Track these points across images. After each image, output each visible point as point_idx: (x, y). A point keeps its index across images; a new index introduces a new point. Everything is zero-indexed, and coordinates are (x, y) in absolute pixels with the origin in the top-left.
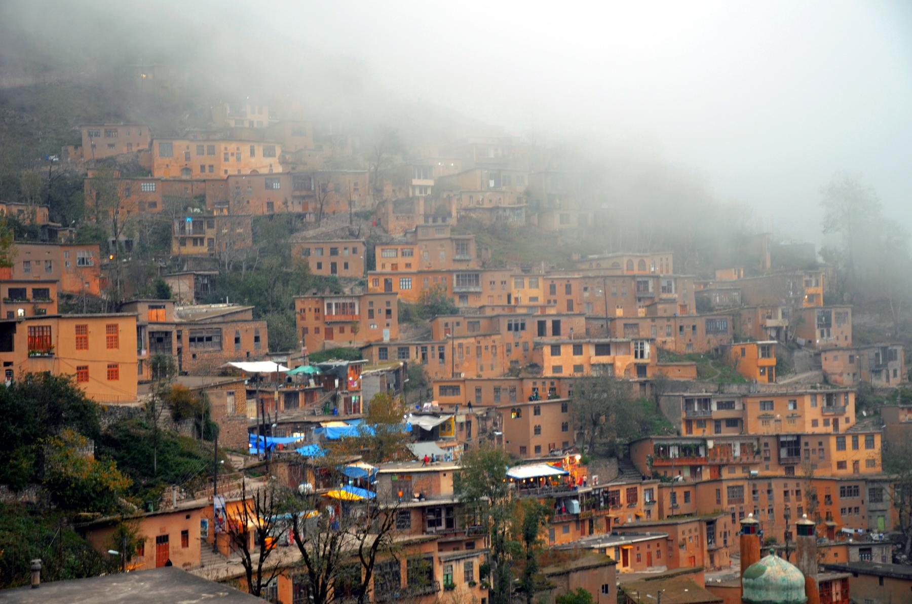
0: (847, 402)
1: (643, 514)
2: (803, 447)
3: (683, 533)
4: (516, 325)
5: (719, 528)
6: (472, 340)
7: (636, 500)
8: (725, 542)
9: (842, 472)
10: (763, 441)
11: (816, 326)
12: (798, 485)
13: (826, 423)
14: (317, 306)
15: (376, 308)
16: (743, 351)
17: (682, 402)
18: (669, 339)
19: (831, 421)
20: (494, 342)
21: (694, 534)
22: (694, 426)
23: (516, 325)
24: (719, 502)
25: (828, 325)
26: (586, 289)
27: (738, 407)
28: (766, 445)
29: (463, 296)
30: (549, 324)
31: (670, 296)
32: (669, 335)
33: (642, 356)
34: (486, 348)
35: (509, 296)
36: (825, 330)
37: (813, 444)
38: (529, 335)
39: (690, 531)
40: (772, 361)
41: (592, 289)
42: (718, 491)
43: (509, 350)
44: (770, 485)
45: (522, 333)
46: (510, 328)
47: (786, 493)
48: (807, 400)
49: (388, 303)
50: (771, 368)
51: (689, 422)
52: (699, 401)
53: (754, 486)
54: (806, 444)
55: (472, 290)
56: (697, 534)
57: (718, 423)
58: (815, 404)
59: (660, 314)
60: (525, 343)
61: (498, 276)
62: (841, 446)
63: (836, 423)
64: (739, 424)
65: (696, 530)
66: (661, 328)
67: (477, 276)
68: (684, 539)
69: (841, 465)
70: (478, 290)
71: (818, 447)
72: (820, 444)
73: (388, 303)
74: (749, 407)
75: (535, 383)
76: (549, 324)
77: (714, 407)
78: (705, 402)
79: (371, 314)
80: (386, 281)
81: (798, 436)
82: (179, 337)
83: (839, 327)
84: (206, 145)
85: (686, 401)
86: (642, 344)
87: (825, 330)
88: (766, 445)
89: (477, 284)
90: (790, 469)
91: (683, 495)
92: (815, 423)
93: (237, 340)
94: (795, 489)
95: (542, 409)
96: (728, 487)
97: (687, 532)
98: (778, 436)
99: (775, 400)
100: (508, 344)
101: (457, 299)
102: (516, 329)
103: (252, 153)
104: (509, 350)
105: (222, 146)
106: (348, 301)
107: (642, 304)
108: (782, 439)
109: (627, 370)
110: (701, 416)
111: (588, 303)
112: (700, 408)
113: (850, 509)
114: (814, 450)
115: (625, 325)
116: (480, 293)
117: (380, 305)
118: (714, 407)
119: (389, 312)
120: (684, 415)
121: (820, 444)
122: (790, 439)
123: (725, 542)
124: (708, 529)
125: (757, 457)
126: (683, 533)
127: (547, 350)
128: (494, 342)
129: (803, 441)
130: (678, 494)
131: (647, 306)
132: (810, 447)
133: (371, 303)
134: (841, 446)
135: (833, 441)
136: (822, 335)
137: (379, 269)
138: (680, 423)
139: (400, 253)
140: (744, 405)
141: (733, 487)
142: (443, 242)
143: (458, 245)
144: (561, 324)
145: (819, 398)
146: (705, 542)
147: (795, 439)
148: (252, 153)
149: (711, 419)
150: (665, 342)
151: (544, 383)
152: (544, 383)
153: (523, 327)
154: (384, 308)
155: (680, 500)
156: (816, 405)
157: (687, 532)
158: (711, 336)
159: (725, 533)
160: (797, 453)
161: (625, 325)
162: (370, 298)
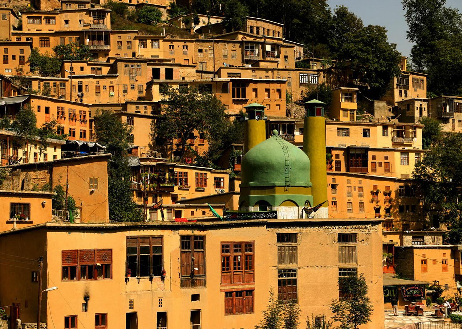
7: (206, 186)
11: (395, 86)
12: (360, 182)
20: (112, 83)
25: (406, 87)
26: (200, 51)
28: (338, 156)
34: (105, 87)
36: (403, 91)
41: (206, 51)
43: (125, 91)
48: (380, 128)
50: (352, 111)
54: (374, 157)
60: (141, 85)
61: (125, 37)
71: (383, 161)
72: (386, 158)
75: (137, 107)
87: (403, 91)
88: (338, 156)
104: (125, 91)
111: (201, 63)
115: (228, 74)
116: (109, 51)
121: (386, 158)
128: (112, 83)
129: (370, 154)
132: (377, 161)
136: (400, 95)
144: (174, 72)
151: (146, 107)
152: (146, 107)
158: (303, 88)
161: (228, 74)
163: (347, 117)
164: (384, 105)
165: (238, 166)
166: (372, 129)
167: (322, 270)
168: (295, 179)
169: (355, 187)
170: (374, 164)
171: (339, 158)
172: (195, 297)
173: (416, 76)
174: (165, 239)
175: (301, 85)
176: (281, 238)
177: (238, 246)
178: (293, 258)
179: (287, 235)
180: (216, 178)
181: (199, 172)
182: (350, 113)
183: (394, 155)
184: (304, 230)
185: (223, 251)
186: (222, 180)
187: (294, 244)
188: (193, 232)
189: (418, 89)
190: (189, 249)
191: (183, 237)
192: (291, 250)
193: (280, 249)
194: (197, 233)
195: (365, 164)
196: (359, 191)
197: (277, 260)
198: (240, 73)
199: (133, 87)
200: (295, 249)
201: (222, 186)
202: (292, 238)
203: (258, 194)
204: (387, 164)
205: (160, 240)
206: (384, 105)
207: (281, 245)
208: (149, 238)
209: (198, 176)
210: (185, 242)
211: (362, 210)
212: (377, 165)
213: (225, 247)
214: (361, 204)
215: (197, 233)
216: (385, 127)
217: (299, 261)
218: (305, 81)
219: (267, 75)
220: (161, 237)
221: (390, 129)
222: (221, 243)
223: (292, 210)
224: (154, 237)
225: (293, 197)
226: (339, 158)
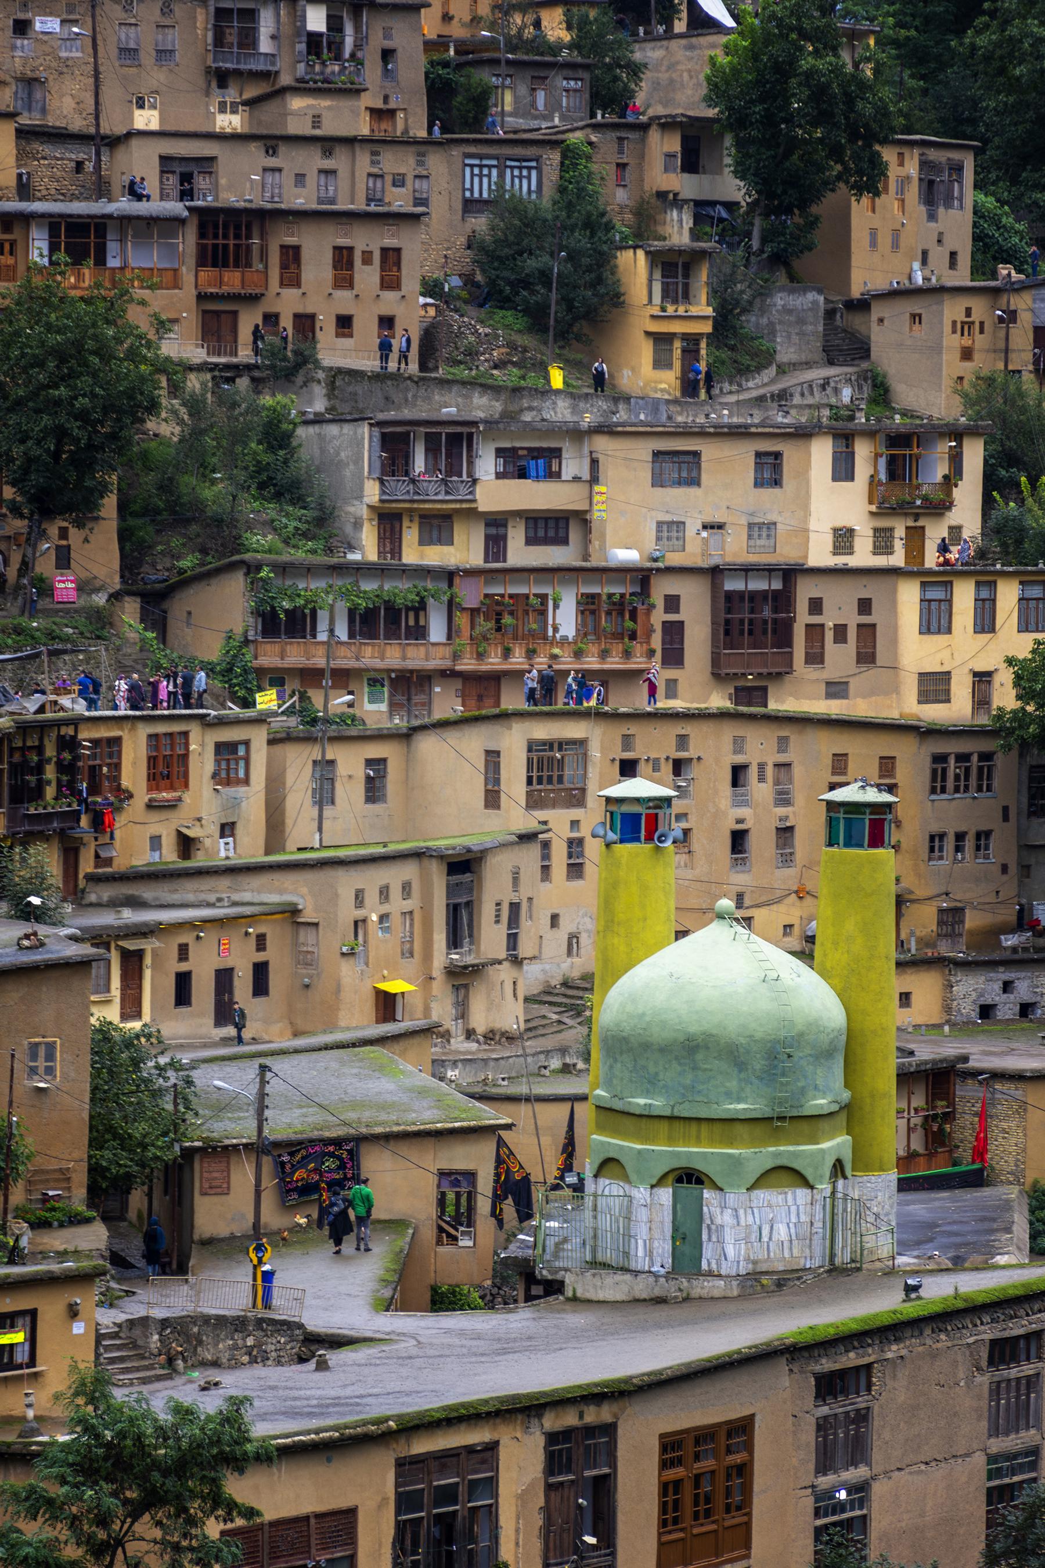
1: (206, 832)
2: (803, 617)
3: (359, 898)
5: (495, 887)
8: (513, 940)
9: (934, 713)
10: (661, 588)
13: (883, 542)
19: (900, 532)
21: (397, 904)
22: (410, 535)
24: (492, 799)
27: (572, 465)
37: (840, 607)
39: (384, 893)
42: (493, 758)
44: (682, 741)
47: (738, 773)
48: (821, 453)
50: (691, 342)
51: (389, 522)
53: (627, 741)
54: (816, 606)
56: (408, 905)
57: (496, 527)
58: (843, 470)
59: (294, 127)
62: (936, 620)
63: (916, 537)
64: (574, 535)
65: (406, 889)
68: (358, 924)
69: (935, 686)
71: (853, 620)
72: (865, 606)
74: (609, 470)
77: (486, 465)
81: (791, 573)
83: (932, 217)
85: (384, 436)
88: (672, 603)
90: (750, 694)
91: (360, 772)
92: (843, 539)
94: (772, 758)
96: (532, 746)
97: (372, 897)
98: (715, 573)
99: (710, 451)
107: (231, 95)
108: (734, 585)
110: (435, 496)
112: (432, 468)
114: (840, 632)
118: (486, 465)
120: (372, 492)
121: (865, 606)
122: (758, 585)
123: (513, 940)
124: (451, 890)
125: (638, 648)
126: (359, 898)
129: (805, 591)
130: (342, 769)
131: (250, 103)
132: (829, 620)
134: (936, 620)
135: (909, 596)
138: (358, 525)
140: (594, 463)
141: (549, 745)
146: (440, 938)
147: (777, 585)
149: (472, 514)
155: (350, 789)
156: (850, 476)
157: (372, 897)
158: (480, 223)
159: (515, 907)
163: (669, 366)
164: (815, 303)
165: (268, 647)
166: (790, 452)
167: (938, 1472)
168: (803, 1091)
169: (762, 767)
170: (815, 632)
171: (677, 611)
173: (933, 154)
175: (470, 206)
176: (829, 1386)
177: (703, 1436)
178: (858, 1451)
179: (842, 1373)
180: (219, 747)
181: (161, 728)
182: (684, 351)
183: (894, 592)
184: (893, 1351)
185: (665, 1465)
186: (241, 752)
187: (861, 1402)
188: (581, 1416)
189: (941, 210)
190: (569, 1471)
191: (552, 1438)
192: (853, 1422)
193: (823, 1426)
194: (593, 1415)
195: (783, 635)
196: (777, 782)
197: (812, 1466)
198: (212, 159)
200: (862, 1417)
201: (241, 774)
202: (857, 1378)
203: (671, 1140)
204: (867, 631)
205: (489, 1453)
206: (815, 303)
207: (825, 1410)
208: (458, 1455)
209: (157, 748)
210: (560, 1451)
211: (787, 859)
212: (829, 636)
214: (785, 832)
215: (593, 1415)
216: (845, 440)
217: (876, 1455)
218: (483, 189)
219: (328, 164)
221: (863, 451)
222: (662, 1436)
223: (790, 1202)
224: (470, 1450)
225: (795, 1155)
226: (677, 611)
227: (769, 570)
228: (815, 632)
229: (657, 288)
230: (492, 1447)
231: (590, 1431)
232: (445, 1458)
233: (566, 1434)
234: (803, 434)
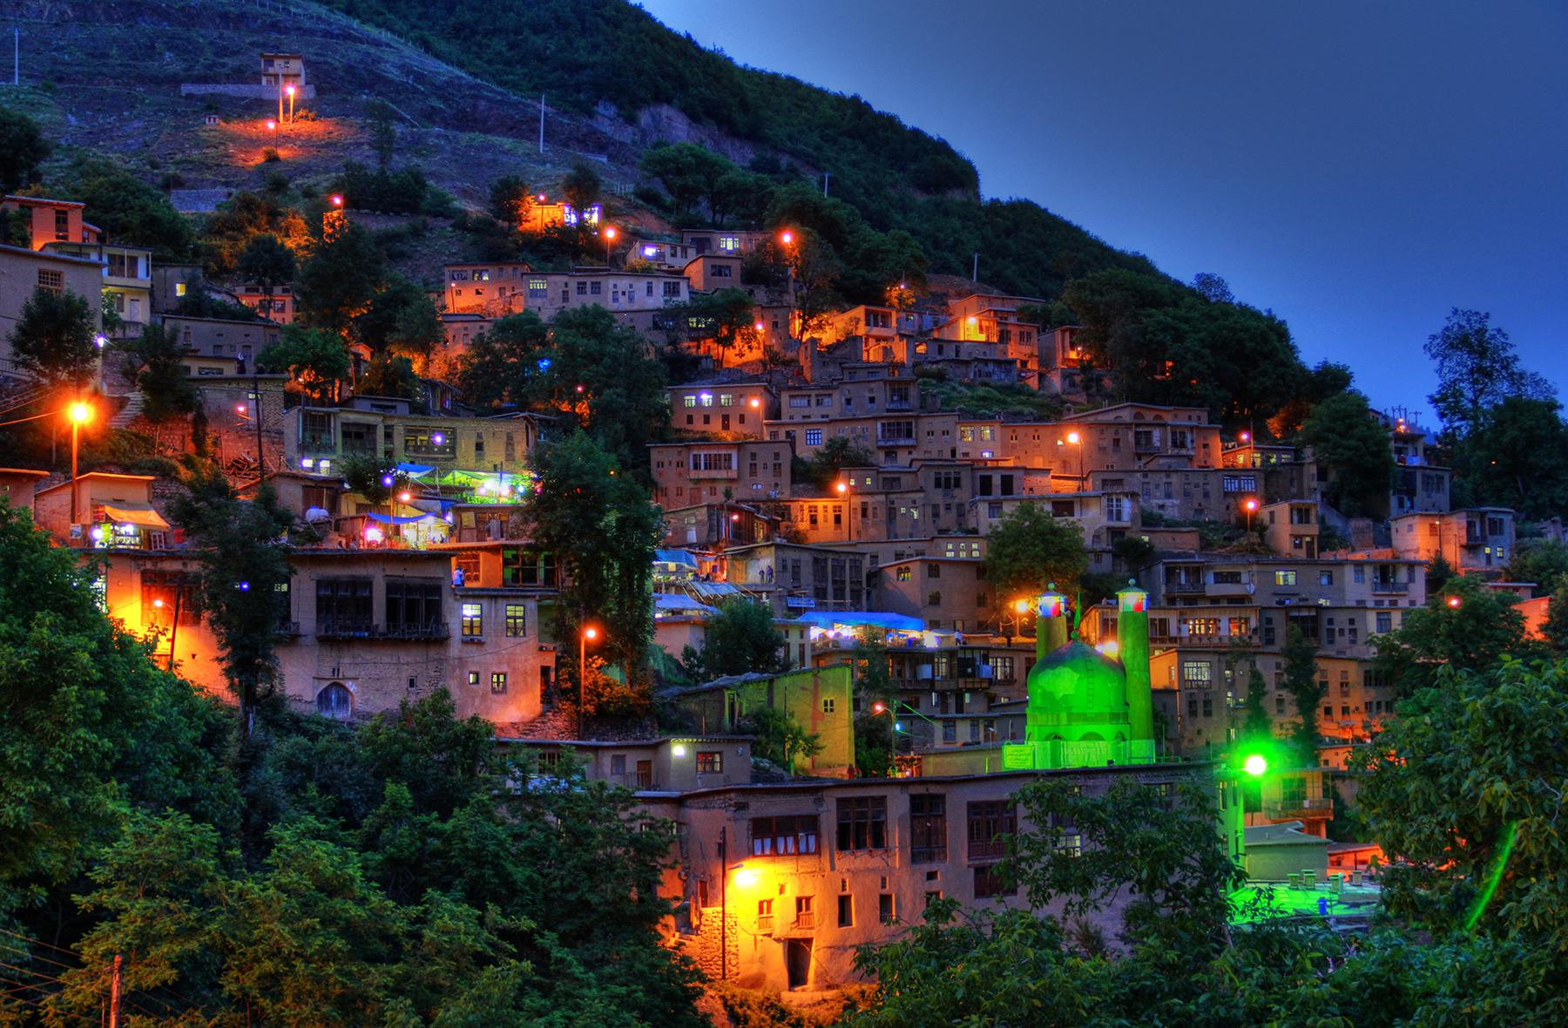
0: (1411, 579)
4: (948, 480)
6: (882, 498)
14: (680, 459)
15: (759, 462)
16: (1272, 513)
17: (1161, 568)
18: (1168, 502)
23: (948, 480)
25: (1411, 493)
29: (891, 452)
30: (997, 480)
31: (1184, 452)
32: (1168, 496)
33: (1119, 518)
35: (953, 452)
38: (962, 495)
40: (1313, 529)
43: (936, 515)
45: (956, 492)
46: (938, 484)
48: (1349, 573)
49: (777, 455)
52: (1187, 570)
54: (1331, 621)
55: (902, 442)
58: (1359, 578)
66: (1157, 486)
67: (910, 424)
70: (910, 442)
71: (1347, 627)
72: (1352, 621)
73: (777, 455)
76: (997, 480)
77: (1210, 578)
78: (1195, 572)
79: (753, 466)
80: (788, 434)
82: (389, 436)
83: (1429, 496)
84: (589, 281)
86: (1118, 500)
89: (909, 435)
93: (479, 447)
95: (943, 569)
100: (935, 507)
101: (882, 455)
102: (947, 486)
103: (650, 291)
104: (936, 515)
105: (611, 281)
106: (723, 452)
109: (1096, 537)
113: (1379, 704)
114: (1342, 631)
117: (765, 456)
118: (1210, 578)
119: (777, 467)
121: (1352, 621)
122: (1305, 613)
127: (983, 509)
133: (754, 456)
136: (1401, 505)
137: (785, 419)
139: (813, 401)
142: (873, 385)
143: (893, 390)
145: (1368, 571)
148: (650, 291)
149: (1204, 597)
150: (1162, 507)
153: (958, 484)
154: (771, 462)
160: (1315, 633)
162: (753, 448)
166: (1335, 570)
172: (931, 876)
174: (889, 802)
191: (913, 798)
199: (948, 507)
210: (917, 803)
213: (973, 807)
215: (934, 790)
220: (884, 797)
227: (1309, 607)
228: (1331, 632)
229: (1295, 518)
230: (884, 797)
231: (933, 797)
232: (861, 801)
233: (921, 796)
234: (1340, 564)
